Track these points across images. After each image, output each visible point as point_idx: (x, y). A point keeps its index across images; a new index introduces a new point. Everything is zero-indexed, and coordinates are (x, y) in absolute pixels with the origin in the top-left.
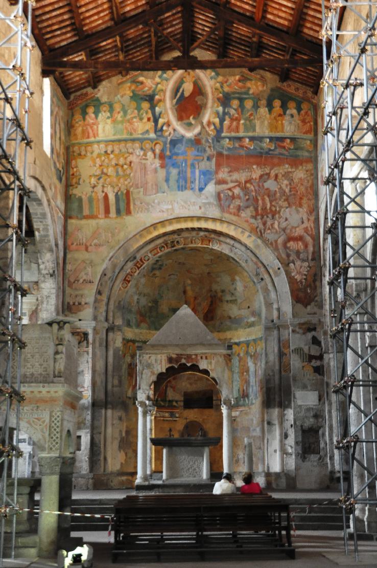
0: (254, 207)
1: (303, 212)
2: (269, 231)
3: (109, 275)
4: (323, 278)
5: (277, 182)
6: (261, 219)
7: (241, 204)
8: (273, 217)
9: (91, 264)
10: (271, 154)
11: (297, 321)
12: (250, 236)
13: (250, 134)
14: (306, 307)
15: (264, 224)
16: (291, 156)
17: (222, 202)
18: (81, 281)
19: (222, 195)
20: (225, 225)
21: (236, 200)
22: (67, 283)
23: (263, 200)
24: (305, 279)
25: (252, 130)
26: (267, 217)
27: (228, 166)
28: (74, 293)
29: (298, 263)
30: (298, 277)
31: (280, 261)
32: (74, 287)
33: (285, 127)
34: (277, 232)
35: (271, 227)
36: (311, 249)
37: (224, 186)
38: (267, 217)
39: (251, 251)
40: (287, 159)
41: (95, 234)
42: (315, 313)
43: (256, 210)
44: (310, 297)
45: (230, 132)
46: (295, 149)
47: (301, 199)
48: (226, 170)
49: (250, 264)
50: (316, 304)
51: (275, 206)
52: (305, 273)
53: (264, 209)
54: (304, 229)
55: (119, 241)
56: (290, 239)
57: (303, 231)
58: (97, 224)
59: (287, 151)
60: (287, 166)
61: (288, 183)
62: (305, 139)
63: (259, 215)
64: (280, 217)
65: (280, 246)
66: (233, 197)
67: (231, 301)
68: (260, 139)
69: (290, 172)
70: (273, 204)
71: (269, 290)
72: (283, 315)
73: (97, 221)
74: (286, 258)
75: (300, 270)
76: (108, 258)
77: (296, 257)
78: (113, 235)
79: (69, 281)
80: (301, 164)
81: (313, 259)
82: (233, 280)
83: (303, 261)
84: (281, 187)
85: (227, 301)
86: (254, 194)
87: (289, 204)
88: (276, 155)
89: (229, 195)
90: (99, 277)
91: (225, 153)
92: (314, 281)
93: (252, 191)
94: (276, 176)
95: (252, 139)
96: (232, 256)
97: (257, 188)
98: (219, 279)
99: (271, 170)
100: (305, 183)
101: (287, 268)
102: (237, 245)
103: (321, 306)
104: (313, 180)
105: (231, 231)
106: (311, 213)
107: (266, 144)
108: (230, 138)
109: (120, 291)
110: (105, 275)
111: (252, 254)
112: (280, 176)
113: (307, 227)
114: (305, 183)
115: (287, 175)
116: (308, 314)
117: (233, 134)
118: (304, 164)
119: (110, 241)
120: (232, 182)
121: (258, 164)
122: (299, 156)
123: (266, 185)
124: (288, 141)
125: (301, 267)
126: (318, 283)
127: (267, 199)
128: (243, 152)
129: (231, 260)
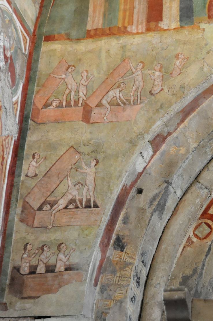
3: (151, 190)
9: (97, 153)
18: (62, 203)
22: (19, 210)
28: (37, 239)
32: (36, 224)
41: (115, 75)
55: (182, 87)
58: (123, 47)
73: (124, 40)
76: (149, 137)
78: (167, 73)
79: (26, 206)
90: (116, 191)
109: (189, 249)
110: (140, 191)
119: (157, 90)
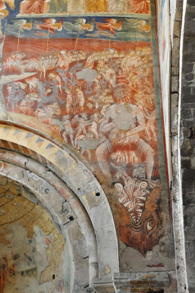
0: (59, 104)
1: (138, 111)
2: (82, 136)
4: (173, 203)
5: (97, 70)
6: (70, 120)
7: (39, 100)
8: (89, 117)
10: (88, 37)
11: (128, 278)
12: (52, 146)
13: (59, 14)
14: (144, 253)
15: (75, 126)
16: (118, 39)
17: (9, 98)
19: (10, 88)
20: (13, 131)
21: (32, 95)
23: (74, 94)
24: (141, 208)
25: (61, 10)
26: (80, 117)
27: (22, 51)
29: (130, 183)
30: (130, 205)
31: (98, 180)
33: (110, 6)
34: (94, 137)
35: (85, 131)
36: (151, 162)
37: (16, 77)
38: (80, 117)
39: (54, 173)
40: (111, 42)
42: (161, 265)
43: (63, 107)
44: (151, 236)
45: (30, 12)
46: (125, 31)
47: (134, 92)
48: (19, 56)
49: (52, 196)
50: (162, 248)
51: (92, 103)
52: (142, 198)
53: (75, 106)
54: (139, 133)
56: (116, 148)
57: (138, 136)
59: (112, 33)
60: (112, 51)
61: (113, 72)
62: (139, 19)
63: (66, 114)
64: (101, 117)
65: (100, 159)
66: (27, 91)
67: (28, 271)
68: (73, 19)
69: (117, 58)
70: (90, 99)
71: (82, 235)
72: (104, 270)
74: (110, 176)
75: (133, 194)
77: (126, 175)
80: (134, 49)
81: (154, 178)
82: (31, 235)
83: (139, 179)
84: (102, 77)
85: (22, 273)
86: (60, 86)
87: (115, 99)
88: (96, 37)
89: (20, 88)
91: (19, 36)
92: (158, 211)
93: (58, 83)
94: (96, 64)
95: (60, 20)
96: (24, 183)
97: (65, 79)
98: (9, 237)
99: (87, 56)
100: (140, 72)
101: (111, 191)
102: (32, 165)
103: (171, 253)
104: (152, 68)
105: (20, 139)
106: (150, 111)
107: (81, 26)
108: (28, 20)
111: (55, 178)
112: (101, 63)
113: (144, 131)
114: (140, 72)
115: (110, 62)
116: (149, 266)
117: (33, 15)
118: (138, 49)
120: (27, 71)
121: (68, 49)
122: (130, 38)
123: (80, 75)
124: (114, 21)
125: (135, 189)
126: (164, 215)
127: (80, 93)
128: (46, 36)
129: (24, 194)
